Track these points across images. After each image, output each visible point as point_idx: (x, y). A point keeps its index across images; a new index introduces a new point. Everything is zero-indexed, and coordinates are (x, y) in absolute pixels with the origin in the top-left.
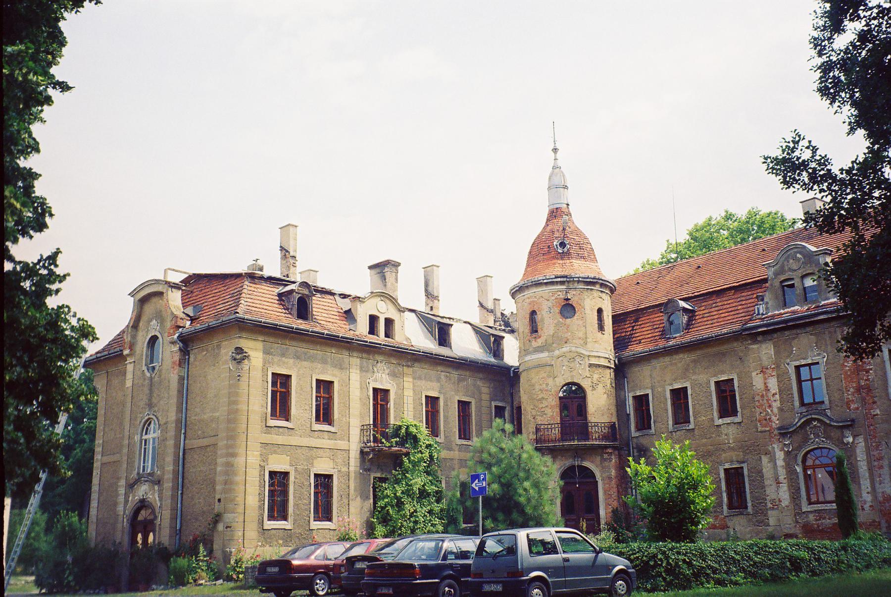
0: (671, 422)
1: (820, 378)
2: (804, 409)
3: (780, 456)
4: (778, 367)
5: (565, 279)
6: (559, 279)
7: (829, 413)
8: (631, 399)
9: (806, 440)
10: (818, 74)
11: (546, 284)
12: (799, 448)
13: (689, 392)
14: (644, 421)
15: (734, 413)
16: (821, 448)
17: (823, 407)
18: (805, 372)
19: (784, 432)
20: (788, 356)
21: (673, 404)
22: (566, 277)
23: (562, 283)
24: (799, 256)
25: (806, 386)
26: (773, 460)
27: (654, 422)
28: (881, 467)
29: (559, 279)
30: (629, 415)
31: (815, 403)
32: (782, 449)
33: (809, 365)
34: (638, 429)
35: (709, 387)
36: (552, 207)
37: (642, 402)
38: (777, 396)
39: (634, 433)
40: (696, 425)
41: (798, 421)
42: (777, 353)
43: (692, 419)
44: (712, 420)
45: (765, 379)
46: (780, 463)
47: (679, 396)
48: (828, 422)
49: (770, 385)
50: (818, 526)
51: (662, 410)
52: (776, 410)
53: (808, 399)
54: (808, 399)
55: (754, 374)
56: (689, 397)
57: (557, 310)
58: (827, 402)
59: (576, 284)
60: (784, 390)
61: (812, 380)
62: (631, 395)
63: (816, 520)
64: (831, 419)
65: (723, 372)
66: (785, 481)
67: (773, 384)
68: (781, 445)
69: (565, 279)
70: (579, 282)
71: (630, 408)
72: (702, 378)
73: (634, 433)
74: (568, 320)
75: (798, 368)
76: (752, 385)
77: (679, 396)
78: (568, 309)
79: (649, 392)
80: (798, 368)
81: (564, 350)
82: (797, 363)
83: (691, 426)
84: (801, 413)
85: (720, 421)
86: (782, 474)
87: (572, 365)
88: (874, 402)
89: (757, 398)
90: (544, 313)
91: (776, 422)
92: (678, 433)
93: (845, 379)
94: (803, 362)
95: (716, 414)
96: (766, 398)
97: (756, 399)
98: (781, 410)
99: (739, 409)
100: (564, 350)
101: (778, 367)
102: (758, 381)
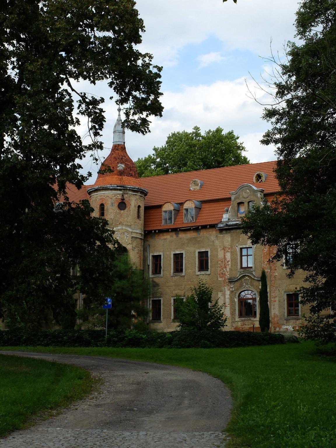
0: (172, 271)
1: (252, 255)
2: (242, 270)
3: (228, 293)
4: (232, 247)
5: (122, 188)
6: (119, 188)
7: (254, 273)
8: (151, 258)
9: (241, 286)
10: (139, 13)
11: (111, 189)
12: (237, 289)
13: (184, 256)
14: (157, 269)
15: (207, 269)
16: (248, 290)
17: (252, 270)
18: (244, 252)
19: (231, 281)
20: (237, 243)
21: (174, 262)
22: (123, 187)
23: (120, 190)
24: (248, 191)
25: (244, 258)
26: (224, 295)
27: (163, 270)
28: (275, 301)
29: (119, 188)
30: (149, 266)
31: (248, 267)
32: (229, 290)
33: (247, 248)
34: (153, 274)
35: (195, 255)
36: (115, 143)
37: (157, 259)
38: (230, 262)
39: (151, 276)
40: (185, 274)
41: (238, 276)
42: (232, 240)
43: (184, 270)
44: (195, 272)
45: (225, 253)
46: (227, 296)
47: (178, 258)
48: (253, 277)
49: (226, 257)
50: (242, 329)
51: (168, 264)
52: (228, 270)
53: (244, 265)
54: (244, 265)
55: (219, 250)
56: (184, 259)
57: (116, 205)
58: (253, 268)
59: (128, 191)
60: (233, 259)
61: (247, 256)
62: (151, 254)
63: (242, 325)
64: (255, 276)
65: (203, 247)
66: (229, 306)
67: (228, 256)
68: (229, 287)
69: (122, 188)
70: (129, 190)
71: (150, 262)
72: (191, 249)
73: (151, 276)
74: (122, 211)
75: (241, 249)
76: (217, 256)
77: (178, 258)
78: (122, 205)
79: (161, 254)
80: (241, 249)
81: (119, 228)
82: (241, 247)
83: (183, 274)
84: (240, 272)
85: (199, 273)
86: (228, 301)
87: (123, 236)
88: (275, 270)
89: (220, 262)
90: (108, 206)
91: (228, 276)
92: (175, 277)
93: (263, 257)
94: (244, 246)
95: (197, 269)
96: (224, 263)
97: (219, 263)
98: (231, 270)
99: (209, 267)
100: (119, 228)
101: (232, 247)
102: (221, 255)
